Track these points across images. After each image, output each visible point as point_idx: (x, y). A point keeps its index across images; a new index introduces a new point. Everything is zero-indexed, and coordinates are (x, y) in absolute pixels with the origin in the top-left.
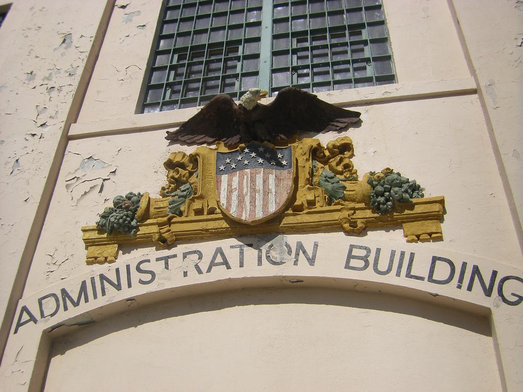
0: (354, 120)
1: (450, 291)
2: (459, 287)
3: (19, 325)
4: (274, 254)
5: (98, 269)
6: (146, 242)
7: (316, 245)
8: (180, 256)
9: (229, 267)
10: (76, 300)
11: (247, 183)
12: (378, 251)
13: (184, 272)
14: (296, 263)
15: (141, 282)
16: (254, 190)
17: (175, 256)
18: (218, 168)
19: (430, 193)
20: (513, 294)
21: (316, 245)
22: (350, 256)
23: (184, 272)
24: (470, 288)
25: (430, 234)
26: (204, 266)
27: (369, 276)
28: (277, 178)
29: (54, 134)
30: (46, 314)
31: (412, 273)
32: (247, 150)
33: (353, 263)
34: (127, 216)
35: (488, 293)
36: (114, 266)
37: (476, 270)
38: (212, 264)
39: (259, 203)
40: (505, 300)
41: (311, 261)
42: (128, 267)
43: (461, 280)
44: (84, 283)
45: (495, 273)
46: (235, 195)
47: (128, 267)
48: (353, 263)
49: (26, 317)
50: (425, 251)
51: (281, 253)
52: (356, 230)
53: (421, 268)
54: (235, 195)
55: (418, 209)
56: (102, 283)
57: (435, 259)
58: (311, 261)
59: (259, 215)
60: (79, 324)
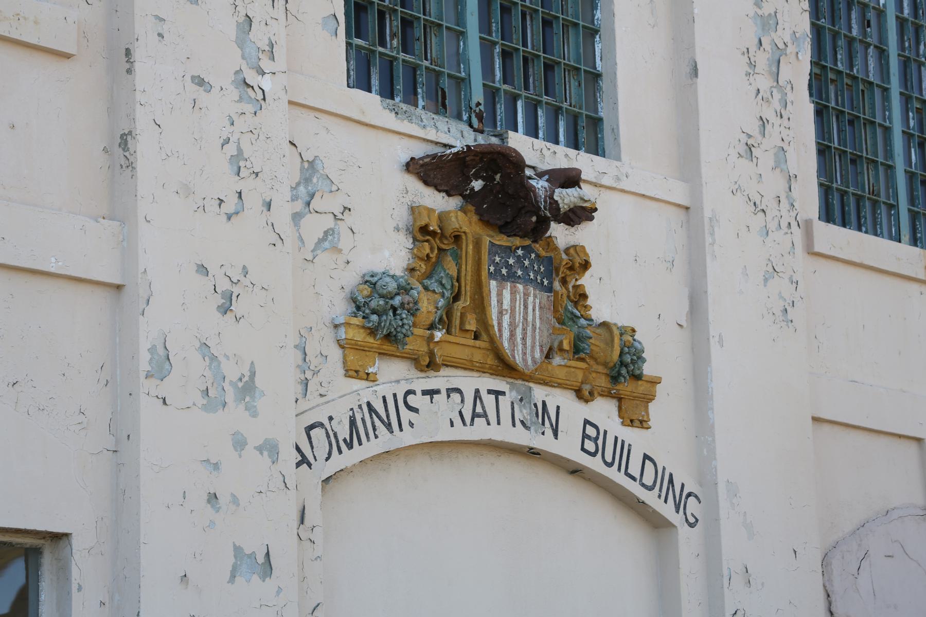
1: (650, 498)
7: (558, 408)
9: (489, 424)
11: (520, 307)
12: (605, 432)
20: (693, 515)
21: (558, 408)
22: (585, 436)
32: (520, 252)
38: (475, 415)
40: (687, 520)
41: (556, 435)
42: (395, 395)
43: (660, 490)
46: (506, 319)
47: (395, 395)
48: (590, 446)
51: (530, 414)
54: (506, 319)
56: (371, 415)
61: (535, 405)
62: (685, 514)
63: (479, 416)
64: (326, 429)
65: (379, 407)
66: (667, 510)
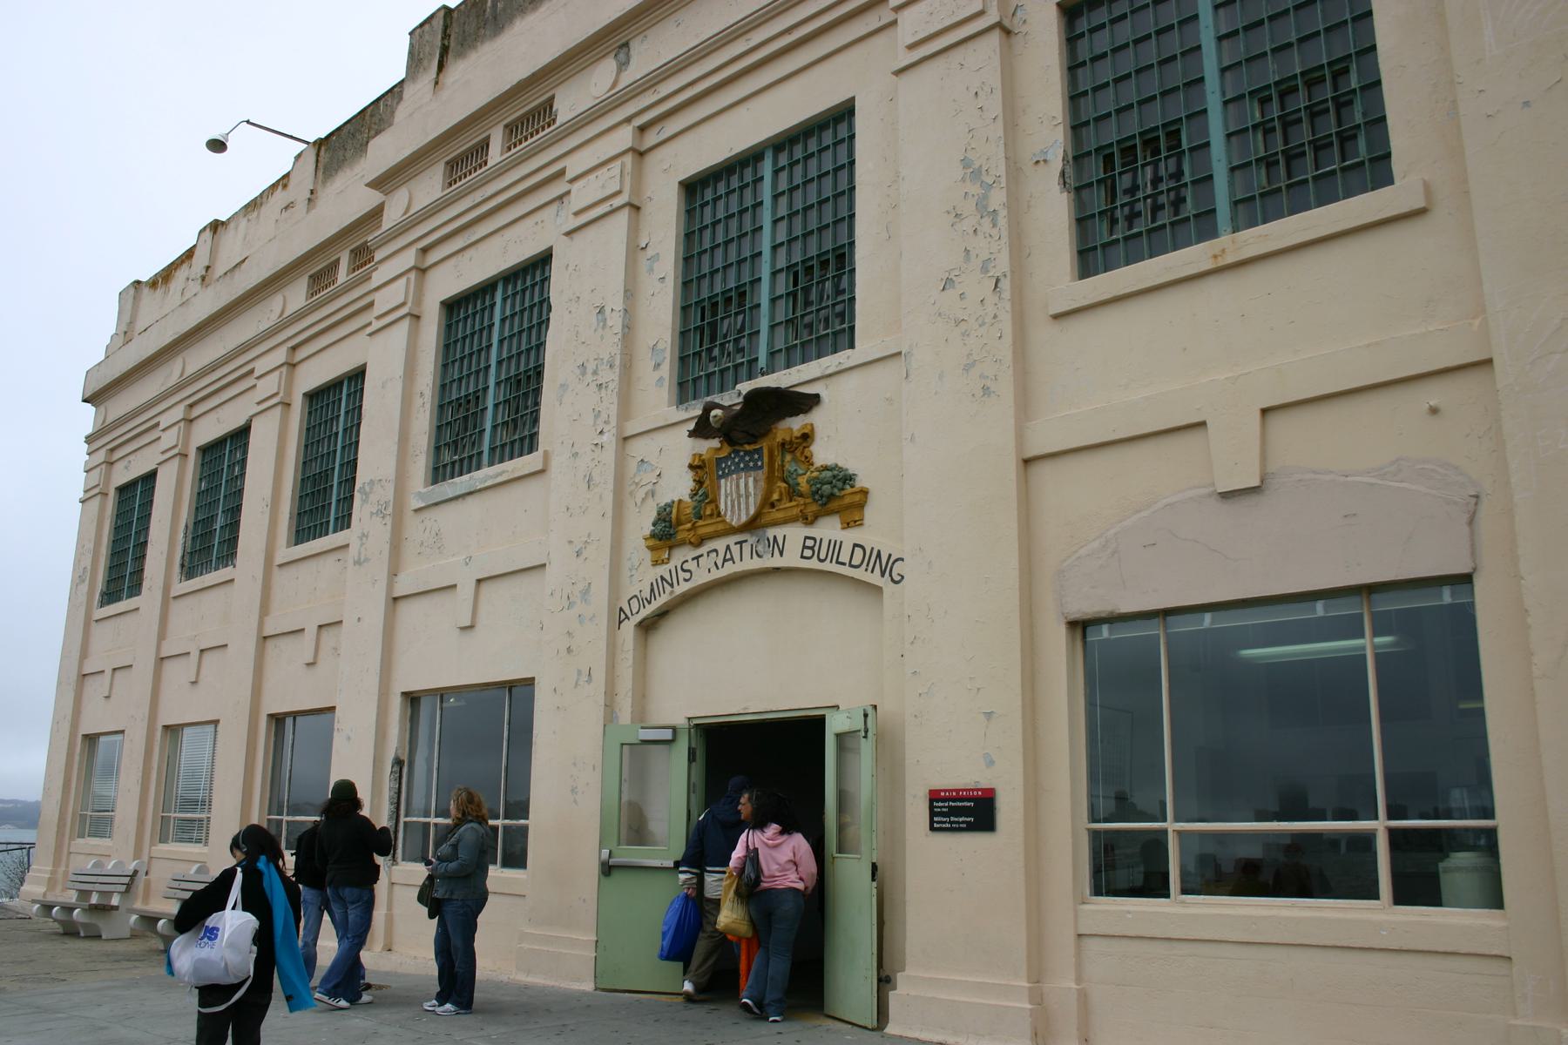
0: (812, 401)
2: (866, 570)
3: (620, 622)
4: (760, 548)
5: (663, 570)
6: (682, 543)
8: (705, 555)
12: (821, 540)
15: (686, 580)
16: (739, 496)
17: (702, 555)
18: (717, 474)
19: (860, 483)
20: (899, 574)
22: (805, 547)
24: (872, 572)
25: (855, 522)
26: (720, 565)
27: (813, 564)
28: (756, 481)
29: (609, 439)
31: (840, 560)
33: (808, 553)
35: (883, 574)
36: (671, 566)
37: (879, 555)
38: (725, 560)
39: (743, 506)
40: (892, 580)
41: (781, 553)
42: (676, 567)
43: (868, 565)
44: (652, 584)
45: (890, 556)
46: (729, 498)
49: (623, 616)
50: (849, 537)
51: (764, 548)
52: (809, 521)
53: (844, 557)
55: (847, 500)
57: (855, 545)
58: (781, 553)
59: (744, 519)
60: (658, 615)
61: (768, 540)
62: (891, 575)
65: (668, 577)
66: (875, 578)
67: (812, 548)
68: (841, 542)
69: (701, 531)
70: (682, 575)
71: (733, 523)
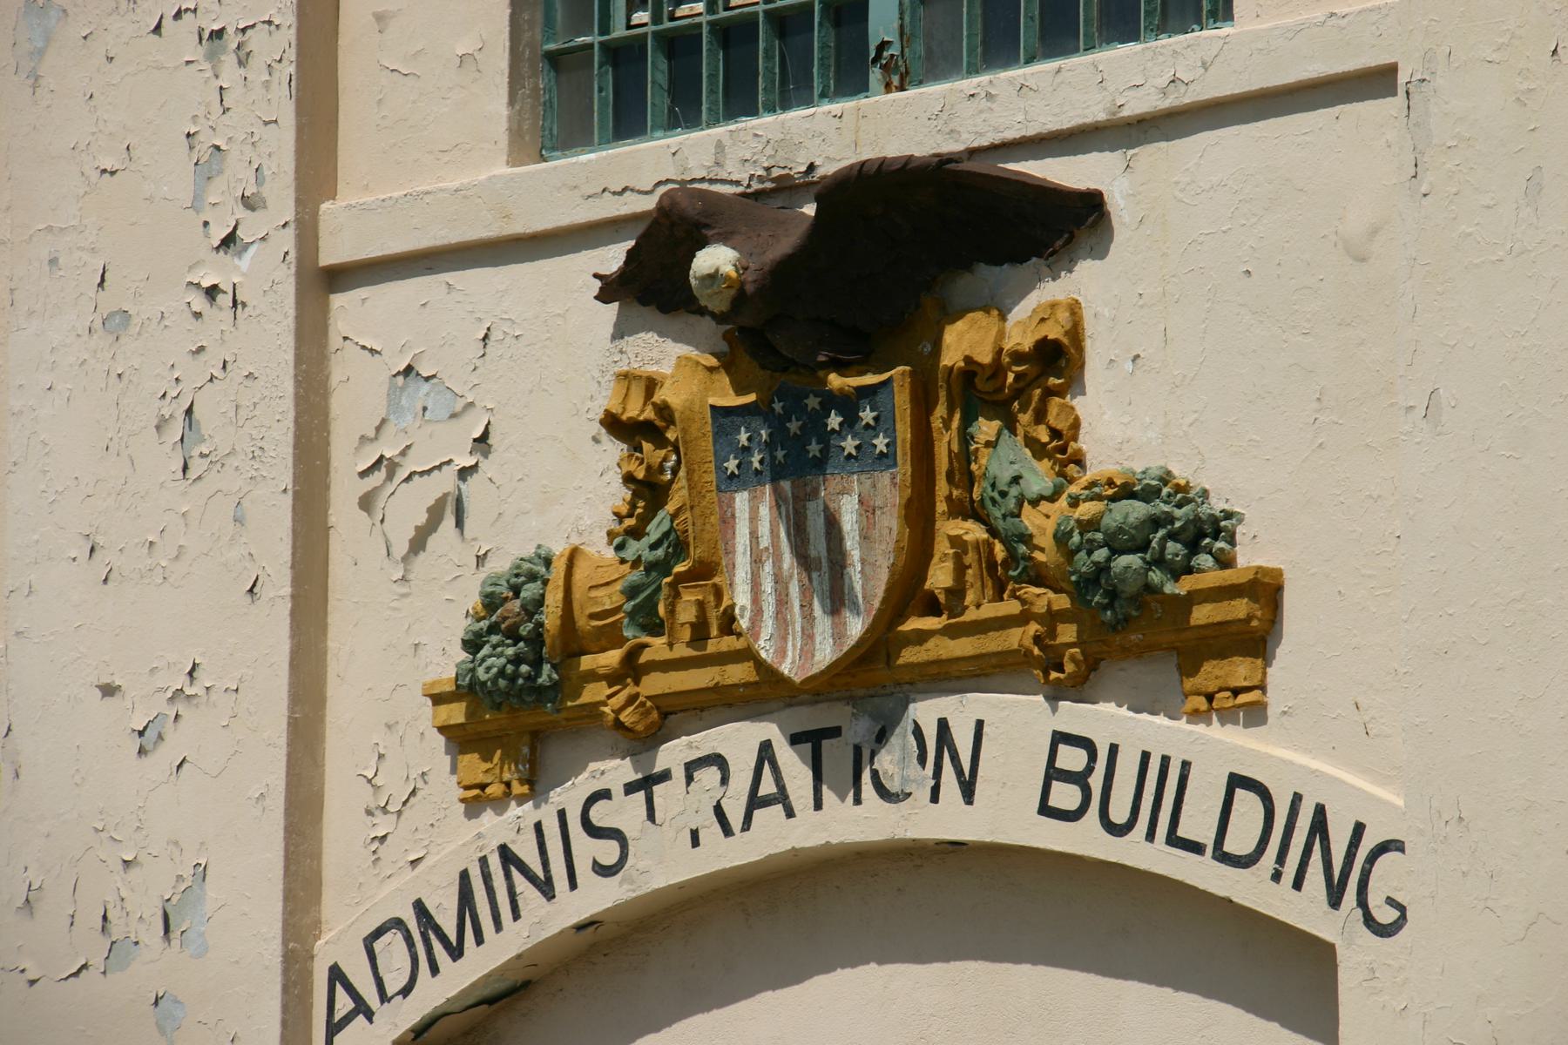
2: (1277, 877)
10: (453, 938)
12: (1114, 750)
13: (691, 830)
14: (935, 798)
18: (720, 469)
20: (1391, 901)
22: (1053, 773)
23: (691, 830)
30: (391, 989)
34: (517, 660)
38: (755, 802)
40: (1369, 920)
43: (1281, 858)
44: (464, 876)
45: (1359, 829)
56: (508, 876)
57: (1237, 782)
62: (1362, 902)
63: (767, 802)
64: (408, 931)
67: (1079, 779)
68: (1186, 765)
69: (655, 684)
70: (587, 849)
71: (785, 669)
